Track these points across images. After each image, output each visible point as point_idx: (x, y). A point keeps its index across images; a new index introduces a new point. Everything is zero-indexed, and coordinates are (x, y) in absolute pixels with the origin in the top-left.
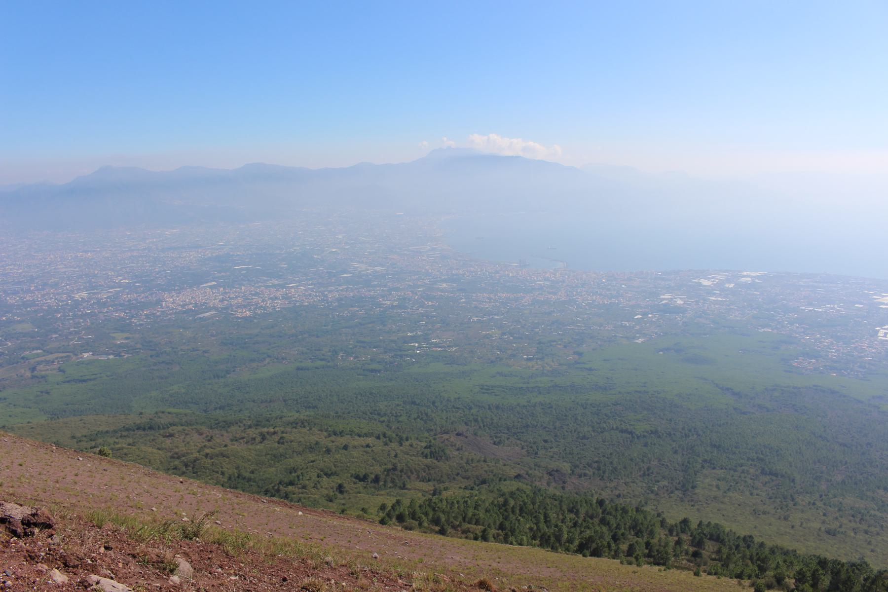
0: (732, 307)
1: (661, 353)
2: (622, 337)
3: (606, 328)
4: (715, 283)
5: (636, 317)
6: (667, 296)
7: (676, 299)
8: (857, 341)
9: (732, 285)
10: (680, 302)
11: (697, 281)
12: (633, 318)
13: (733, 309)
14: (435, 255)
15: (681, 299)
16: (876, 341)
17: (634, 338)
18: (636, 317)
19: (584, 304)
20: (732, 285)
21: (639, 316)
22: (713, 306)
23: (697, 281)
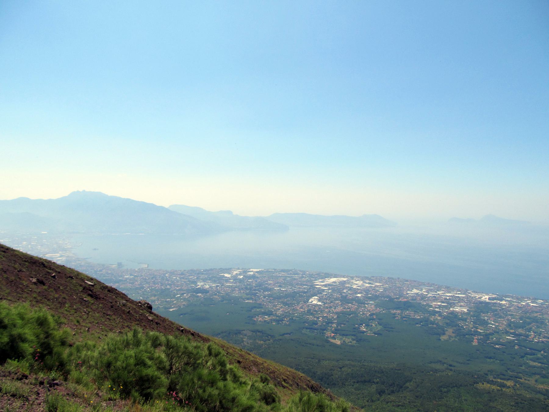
0: (236, 289)
1: (182, 316)
2: (162, 308)
3: (156, 303)
4: (233, 275)
5: (176, 296)
6: (202, 284)
7: (206, 285)
8: (295, 306)
9: (242, 277)
10: (207, 287)
11: (222, 274)
12: (175, 297)
13: (236, 290)
14: (63, 260)
15: (209, 285)
16: (306, 305)
17: (170, 308)
18: (176, 296)
19: (148, 289)
20: (242, 277)
21: (179, 295)
22: (225, 289)
23: (222, 274)
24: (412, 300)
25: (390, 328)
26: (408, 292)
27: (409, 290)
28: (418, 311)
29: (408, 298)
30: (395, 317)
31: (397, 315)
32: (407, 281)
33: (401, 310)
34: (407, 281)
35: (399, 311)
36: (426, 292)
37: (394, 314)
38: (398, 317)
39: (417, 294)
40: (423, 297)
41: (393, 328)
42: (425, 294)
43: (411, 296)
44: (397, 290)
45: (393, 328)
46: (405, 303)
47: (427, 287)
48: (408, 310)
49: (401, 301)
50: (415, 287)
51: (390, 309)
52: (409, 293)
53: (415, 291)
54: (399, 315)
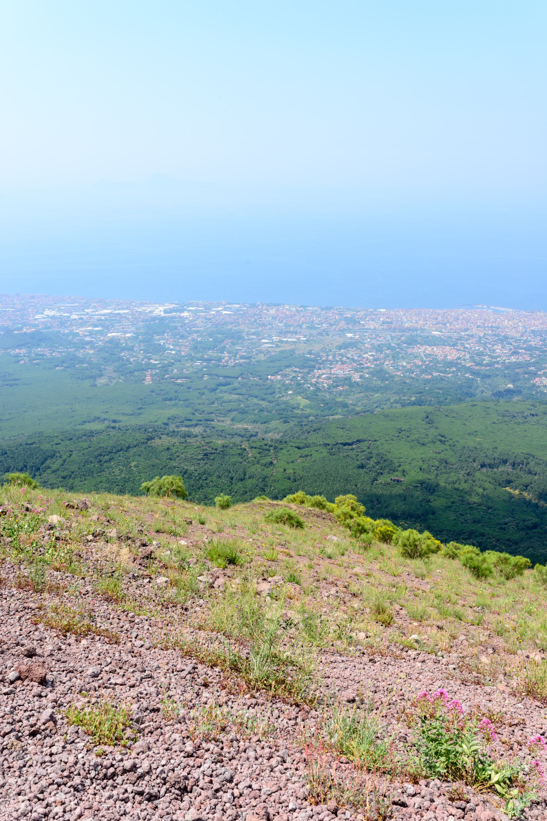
24: (45, 328)
25: (12, 380)
26: (37, 317)
27: (37, 313)
28: (57, 345)
29: (35, 326)
30: (20, 361)
31: (21, 357)
32: (33, 297)
33: (29, 347)
34: (33, 297)
35: (23, 351)
36: (68, 313)
37: (17, 356)
38: (23, 360)
39: (53, 317)
40: (63, 322)
41: (17, 380)
42: (65, 316)
43: (43, 323)
44: (17, 316)
45: (17, 380)
46: (33, 336)
47: (69, 303)
48: (39, 346)
49: (25, 333)
50: (48, 307)
51: (7, 349)
52: (36, 319)
53: (47, 312)
54: (25, 356)
